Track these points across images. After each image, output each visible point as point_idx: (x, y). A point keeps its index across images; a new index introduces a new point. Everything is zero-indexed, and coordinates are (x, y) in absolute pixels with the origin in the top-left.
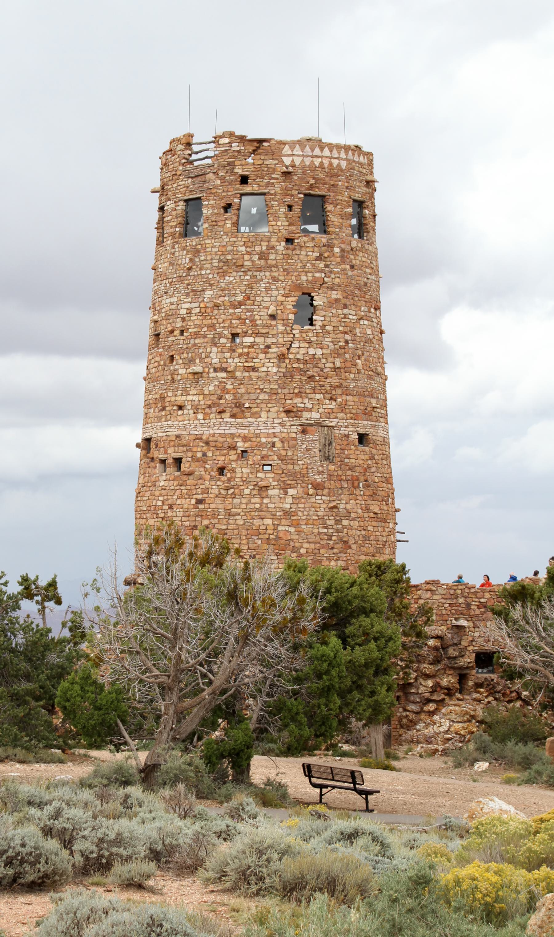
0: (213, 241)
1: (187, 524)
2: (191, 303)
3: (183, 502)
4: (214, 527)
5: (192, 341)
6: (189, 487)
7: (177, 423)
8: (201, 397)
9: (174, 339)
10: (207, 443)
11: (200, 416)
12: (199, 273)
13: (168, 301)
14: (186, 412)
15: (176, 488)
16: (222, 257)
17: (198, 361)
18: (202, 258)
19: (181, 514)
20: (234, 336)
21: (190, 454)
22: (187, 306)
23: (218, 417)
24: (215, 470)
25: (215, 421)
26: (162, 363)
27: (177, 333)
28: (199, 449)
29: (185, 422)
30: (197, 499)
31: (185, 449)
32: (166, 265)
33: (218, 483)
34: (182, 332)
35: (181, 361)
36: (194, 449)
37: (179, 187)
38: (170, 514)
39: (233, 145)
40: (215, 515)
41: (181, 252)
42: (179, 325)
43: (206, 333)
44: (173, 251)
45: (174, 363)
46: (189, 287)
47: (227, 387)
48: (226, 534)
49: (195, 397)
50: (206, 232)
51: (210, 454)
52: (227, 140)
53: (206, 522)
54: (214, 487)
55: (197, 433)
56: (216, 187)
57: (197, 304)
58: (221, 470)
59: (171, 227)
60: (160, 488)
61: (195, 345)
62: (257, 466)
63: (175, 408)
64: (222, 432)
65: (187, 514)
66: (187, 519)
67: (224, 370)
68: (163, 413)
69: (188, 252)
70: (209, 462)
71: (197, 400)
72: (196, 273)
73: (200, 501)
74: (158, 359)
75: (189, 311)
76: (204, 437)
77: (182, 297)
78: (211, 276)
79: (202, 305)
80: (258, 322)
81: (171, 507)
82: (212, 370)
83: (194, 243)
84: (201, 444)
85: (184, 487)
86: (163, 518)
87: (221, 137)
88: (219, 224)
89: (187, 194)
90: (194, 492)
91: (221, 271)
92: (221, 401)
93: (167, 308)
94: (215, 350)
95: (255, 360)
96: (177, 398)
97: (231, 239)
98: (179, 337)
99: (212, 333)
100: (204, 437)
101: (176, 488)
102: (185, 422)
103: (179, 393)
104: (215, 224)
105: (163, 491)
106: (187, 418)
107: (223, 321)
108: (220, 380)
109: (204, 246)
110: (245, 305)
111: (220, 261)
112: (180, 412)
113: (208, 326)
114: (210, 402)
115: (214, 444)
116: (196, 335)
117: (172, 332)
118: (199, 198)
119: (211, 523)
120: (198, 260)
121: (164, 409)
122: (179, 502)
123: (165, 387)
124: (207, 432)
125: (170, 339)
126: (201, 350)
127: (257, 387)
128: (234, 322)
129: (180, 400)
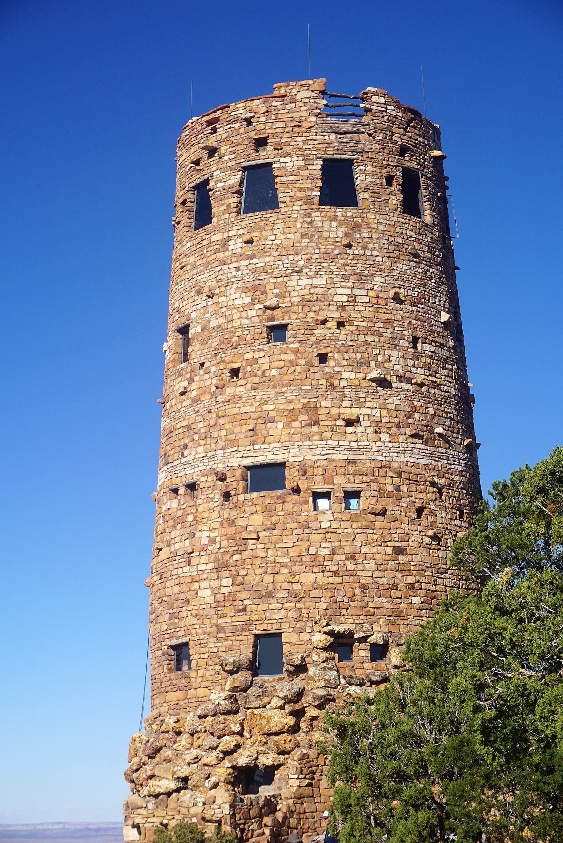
0: (378, 216)
1: (383, 581)
2: (353, 288)
3: (374, 550)
4: (421, 589)
5: (361, 338)
6: (380, 531)
7: (346, 443)
8: (384, 412)
9: (326, 331)
10: (400, 474)
11: (385, 437)
12: (362, 252)
13: (309, 282)
14: (360, 429)
15: (356, 531)
16: (391, 239)
17: (373, 364)
18: (366, 235)
19: (374, 567)
20: (415, 341)
21: (375, 486)
22: (348, 291)
23: (410, 440)
24: (413, 510)
25: (406, 446)
26: (303, 362)
27: (332, 324)
28: (389, 481)
29: (360, 444)
30: (394, 548)
31: (365, 478)
32: (291, 236)
33: (419, 528)
34: (340, 325)
35: (345, 362)
36: (382, 480)
37: (311, 142)
38: (351, 567)
39: (389, 107)
40: (421, 571)
41: (326, 224)
42: (337, 314)
43: (382, 330)
44: (309, 220)
45: (332, 363)
46: (348, 268)
47: (416, 403)
48: (435, 598)
49: (374, 412)
50: (367, 203)
51: (404, 488)
52: (382, 100)
53: (410, 580)
54: (416, 533)
55: (384, 459)
56: (375, 152)
57: (364, 292)
58: (420, 511)
59: (300, 190)
60: (323, 531)
61: (366, 343)
62: (454, 511)
63: (340, 423)
64: (416, 461)
65: (383, 567)
66: (381, 574)
67: (409, 381)
68: (315, 429)
69: (340, 224)
70: (404, 499)
71: (378, 414)
72: (357, 252)
73: (399, 551)
74: (292, 357)
75: (353, 299)
76: (395, 465)
77: (335, 280)
78: (379, 259)
79: (371, 293)
80: (434, 328)
81: (352, 557)
82: (395, 379)
83: (349, 214)
84: (391, 474)
85: (371, 531)
86: (335, 573)
87: (374, 94)
88: (384, 197)
89: (331, 153)
90: (388, 538)
91: (391, 255)
92: (410, 421)
93: (302, 292)
94: (395, 353)
95: (437, 375)
96: (341, 410)
97: (400, 219)
98: (338, 331)
99: (389, 331)
100: (395, 465)
101: (356, 531)
102: (360, 444)
103: (345, 404)
104: (377, 196)
105: (328, 536)
106: (364, 438)
107: (403, 318)
108: (406, 393)
109: (366, 220)
110: (422, 304)
111: (389, 243)
112: (350, 429)
113: (384, 321)
114: (397, 420)
115: (407, 476)
116: (367, 330)
117: (324, 322)
118: (350, 162)
119: (418, 581)
120: (359, 236)
121: (317, 423)
122: (364, 550)
123: (315, 395)
124: (398, 460)
125: (316, 332)
126: (375, 352)
127: (443, 409)
128: (414, 322)
129: (351, 413)
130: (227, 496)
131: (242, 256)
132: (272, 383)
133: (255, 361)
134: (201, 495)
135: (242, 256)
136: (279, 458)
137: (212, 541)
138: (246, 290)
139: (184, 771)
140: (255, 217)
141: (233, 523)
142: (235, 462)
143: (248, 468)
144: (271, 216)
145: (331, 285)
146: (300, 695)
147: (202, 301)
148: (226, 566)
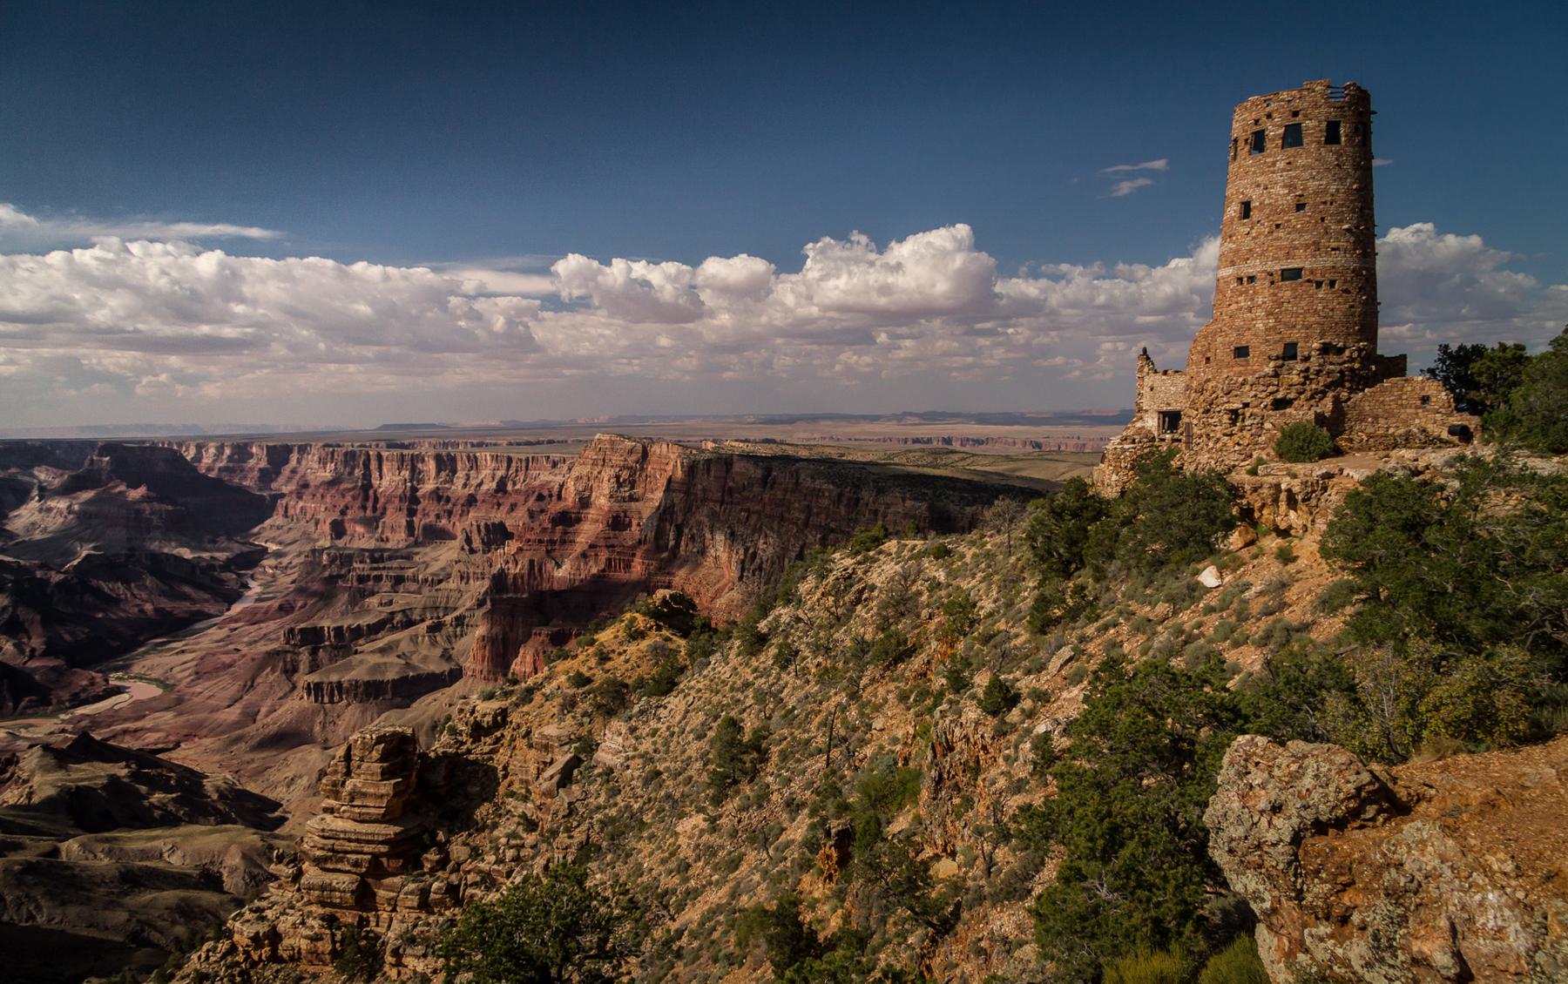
75: (1337, 190)
130: (1272, 283)
131: (1283, 170)
132: (1299, 231)
133: (1289, 221)
134: (1257, 285)
135: (1283, 170)
136: (1301, 265)
137: (1264, 303)
138: (1285, 186)
139: (1249, 400)
140: (1291, 151)
141: (1276, 295)
142: (1277, 268)
143: (1283, 271)
144: (1298, 149)
145: (1328, 184)
146: (1307, 370)
147: (1259, 191)
148: (1272, 314)
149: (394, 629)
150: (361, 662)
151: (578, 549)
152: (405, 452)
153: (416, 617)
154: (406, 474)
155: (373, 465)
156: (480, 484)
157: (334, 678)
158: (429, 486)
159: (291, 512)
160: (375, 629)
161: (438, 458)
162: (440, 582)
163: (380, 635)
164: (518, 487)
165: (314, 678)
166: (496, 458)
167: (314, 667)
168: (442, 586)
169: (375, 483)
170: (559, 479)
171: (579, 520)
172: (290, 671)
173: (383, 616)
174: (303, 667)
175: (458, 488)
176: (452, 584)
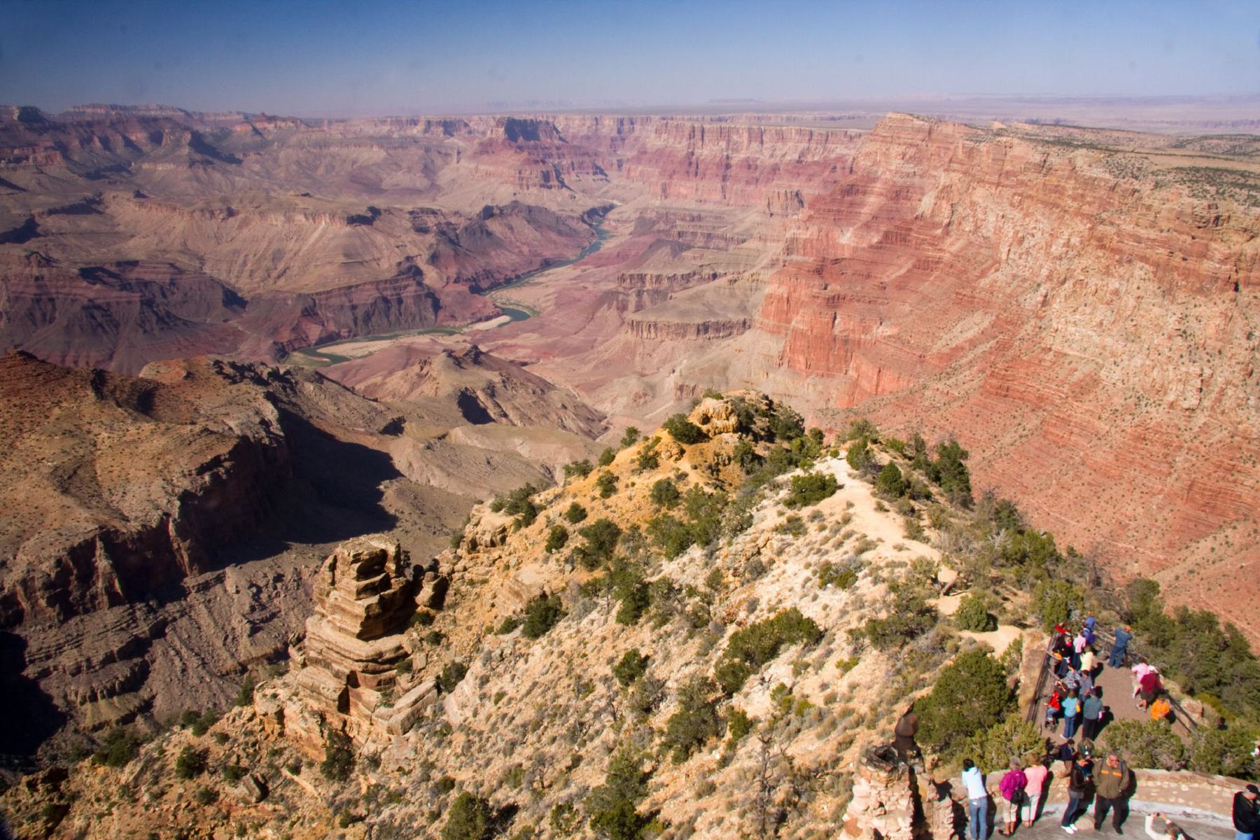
149: (702, 280)
150: (674, 307)
151: (864, 218)
152: (724, 125)
153: (720, 271)
154: (723, 144)
155: (698, 134)
156: (784, 155)
157: (652, 319)
158: (742, 155)
159: (632, 174)
160: (687, 278)
161: (750, 130)
162: (744, 241)
163: (690, 285)
164: (816, 159)
165: (637, 317)
166: (800, 132)
167: (639, 308)
168: (744, 245)
169: (698, 152)
170: (853, 152)
171: (865, 193)
172: (623, 308)
173: (694, 268)
174: (632, 306)
175: (765, 157)
176: (752, 244)
